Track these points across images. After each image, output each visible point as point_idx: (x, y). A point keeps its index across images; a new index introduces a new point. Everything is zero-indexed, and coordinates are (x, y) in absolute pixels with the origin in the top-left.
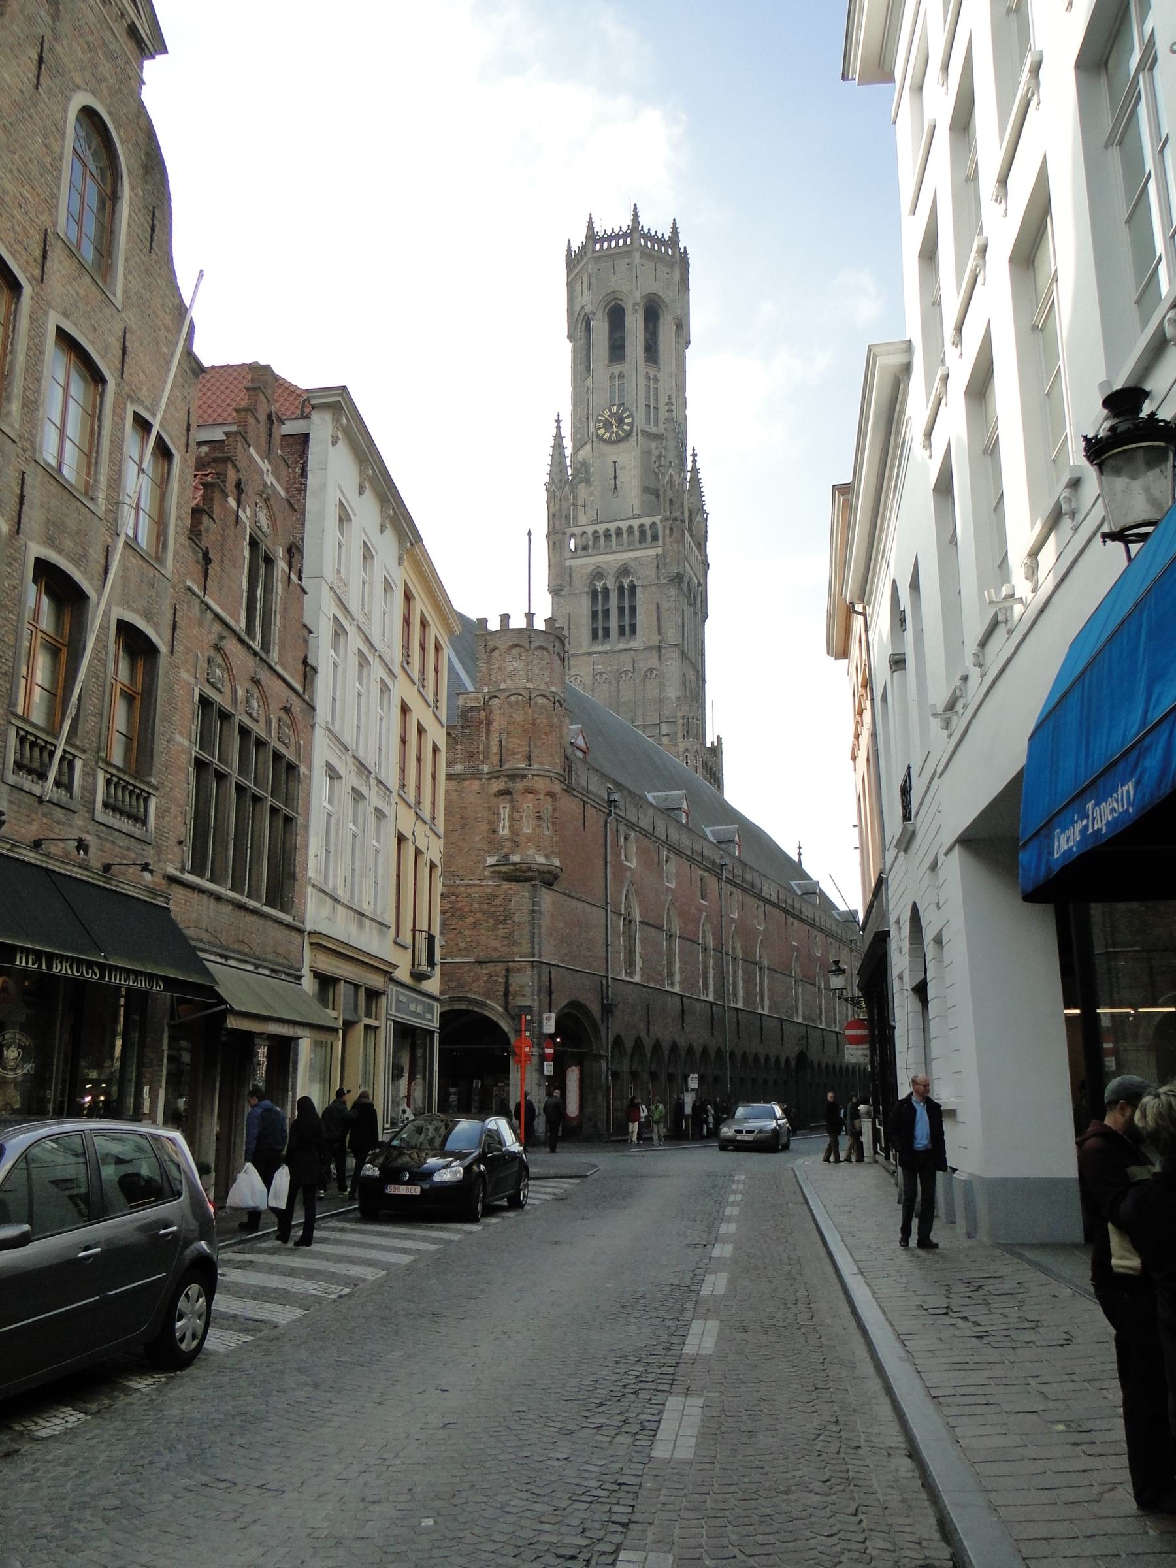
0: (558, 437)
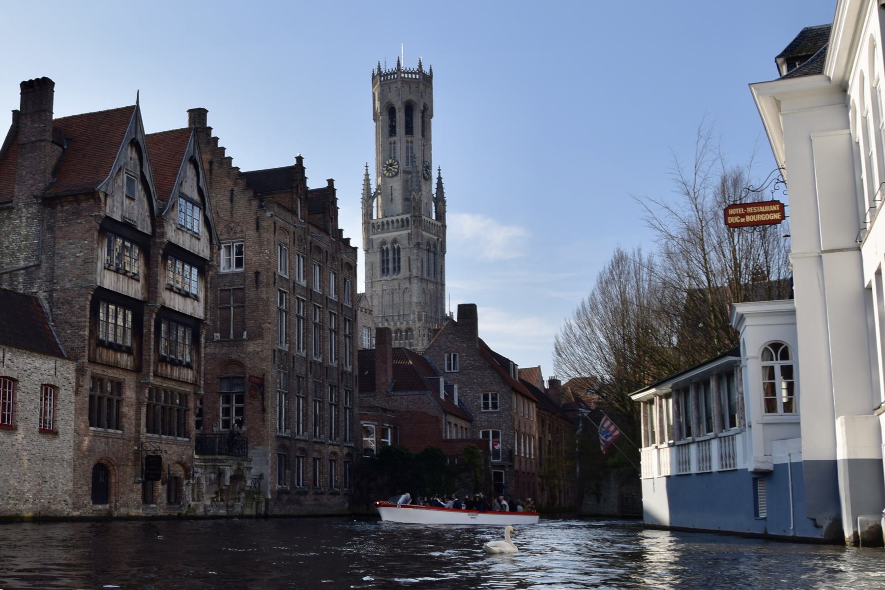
0: (367, 175)
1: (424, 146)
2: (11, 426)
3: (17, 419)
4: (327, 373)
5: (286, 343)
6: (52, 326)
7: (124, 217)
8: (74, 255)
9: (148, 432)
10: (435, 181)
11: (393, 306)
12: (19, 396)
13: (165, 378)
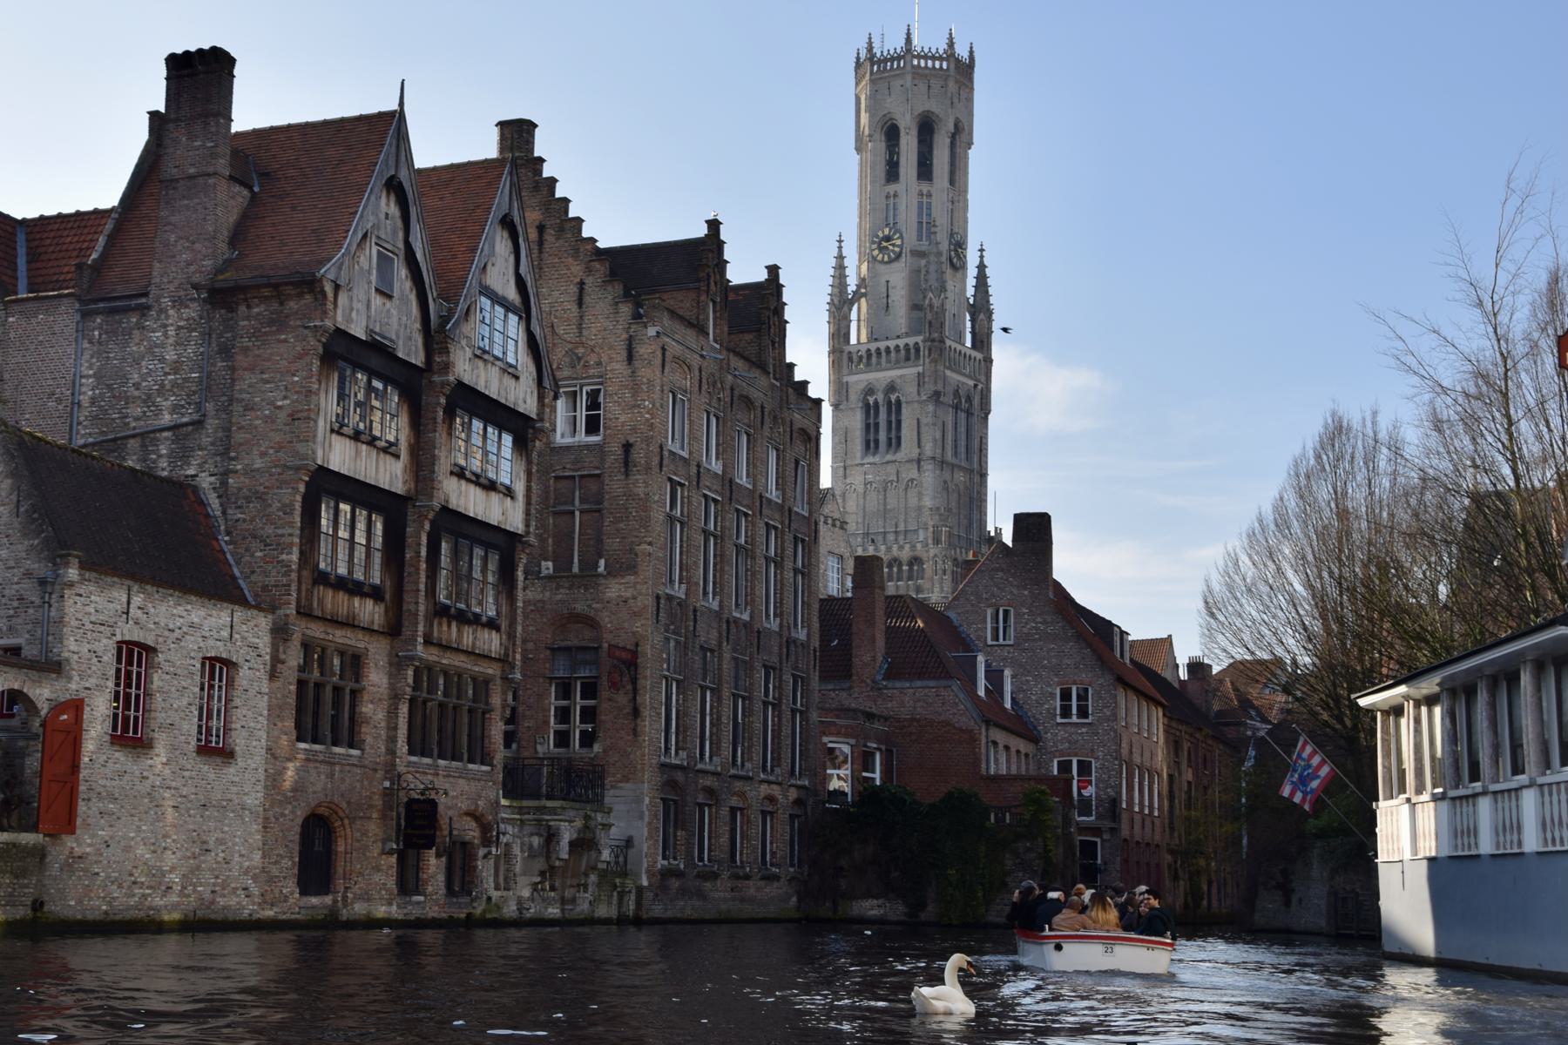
0: (840, 257)
1: (953, 202)
2: (141, 738)
3: (154, 725)
4: (759, 642)
5: (680, 583)
6: (226, 542)
7: (372, 331)
8: (272, 403)
9: (411, 752)
10: (972, 272)
11: (885, 513)
12: (157, 680)
13: (445, 647)
